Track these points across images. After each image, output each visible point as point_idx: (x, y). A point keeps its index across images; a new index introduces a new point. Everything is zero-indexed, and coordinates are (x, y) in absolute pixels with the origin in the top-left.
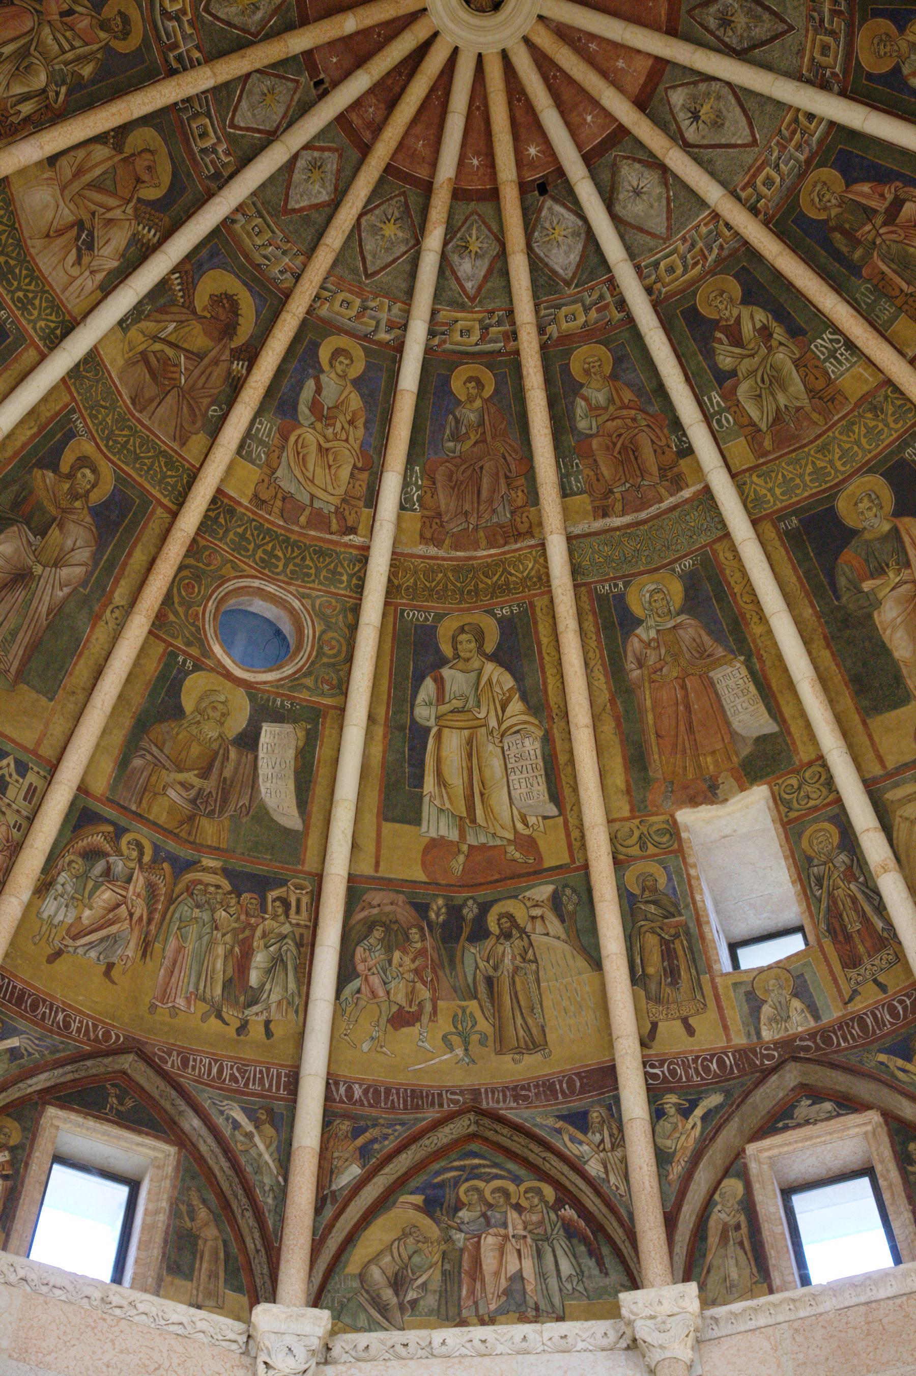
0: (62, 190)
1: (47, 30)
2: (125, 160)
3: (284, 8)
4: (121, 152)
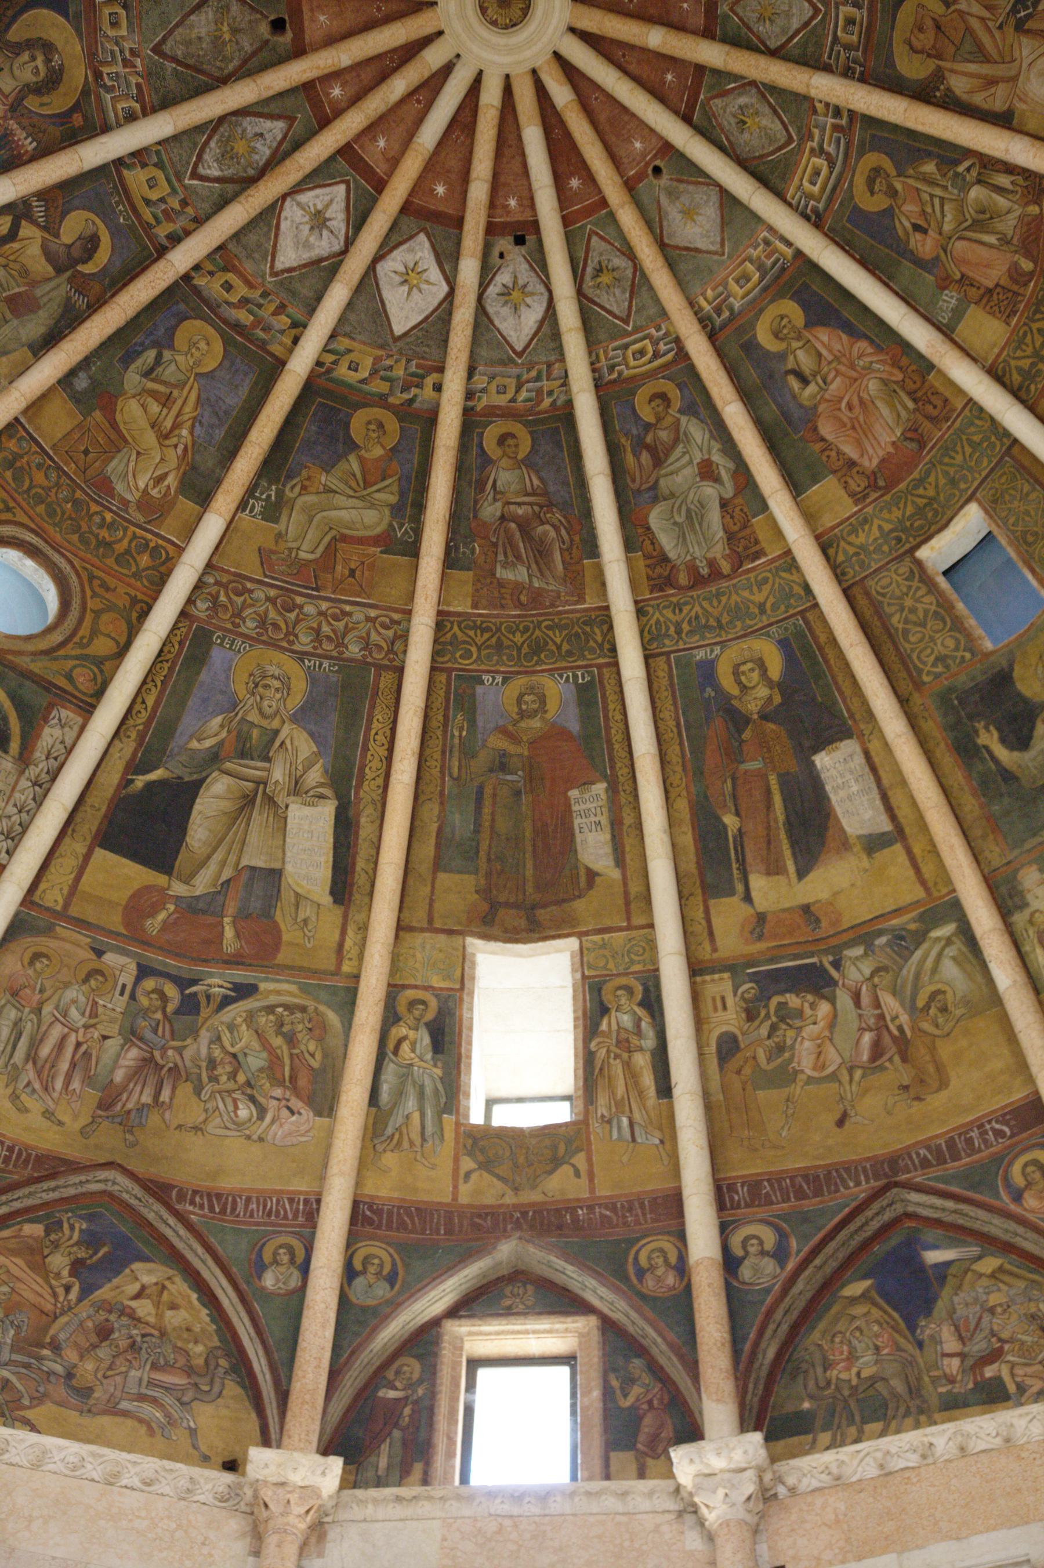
0: (1014, 79)
1: (947, 227)
2: (939, 57)
3: (715, 92)
4: (939, 69)
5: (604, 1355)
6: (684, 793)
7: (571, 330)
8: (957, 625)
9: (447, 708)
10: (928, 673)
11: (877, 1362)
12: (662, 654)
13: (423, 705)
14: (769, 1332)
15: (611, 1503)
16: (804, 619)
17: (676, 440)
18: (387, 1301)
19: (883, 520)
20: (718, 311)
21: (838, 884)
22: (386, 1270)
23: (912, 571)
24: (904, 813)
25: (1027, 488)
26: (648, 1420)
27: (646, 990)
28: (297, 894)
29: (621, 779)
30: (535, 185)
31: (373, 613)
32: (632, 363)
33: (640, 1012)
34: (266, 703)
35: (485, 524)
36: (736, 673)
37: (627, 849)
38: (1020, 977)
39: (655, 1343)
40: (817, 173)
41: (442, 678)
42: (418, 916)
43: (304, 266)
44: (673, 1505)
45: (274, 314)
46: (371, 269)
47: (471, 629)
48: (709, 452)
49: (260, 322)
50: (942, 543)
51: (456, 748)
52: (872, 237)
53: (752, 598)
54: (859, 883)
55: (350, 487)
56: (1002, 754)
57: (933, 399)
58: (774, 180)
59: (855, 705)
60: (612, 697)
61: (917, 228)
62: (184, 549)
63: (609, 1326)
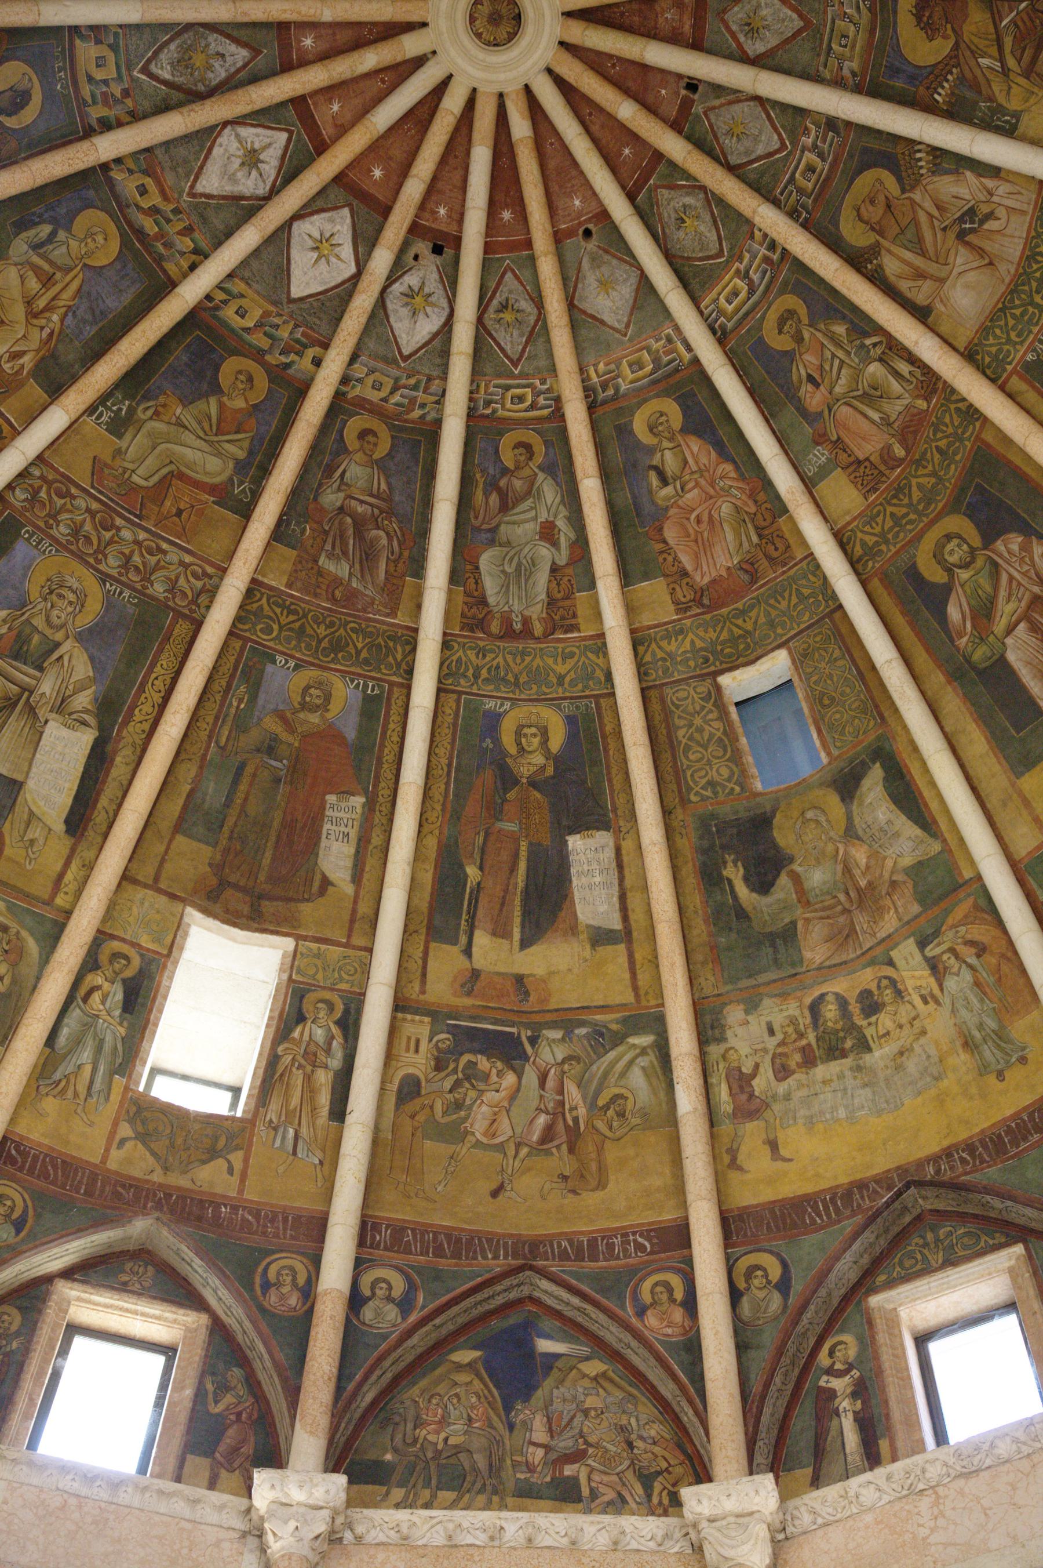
0: (942, 281)
1: (838, 390)
2: (881, 233)
5: (206, 1356)
6: (437, 832)
7: (462, 353)
8: (736, 757)
9: (232, 676)
10: (697, 794)
11: (466, 1433)
12: (453, 692)
13: (211, 666)
14: (374, 1377)
15: (179, 1507)
16: (597, 704)
17: (528, 493)
18: (9, 1246)
19: (697, 637)
20: (604, 386)
21: (557, 965)
22: (15, 1216)
23: (710, 692)
24: (637, 916)
25: (837, 653)
26: (231, 1432)
27: (347, 1011)
28: (31, 813)
29: (381, 799)
30: (469, 203)
31: (188, 559)
32: (509, 405)
33: (335, 1030)
34: (55, 612)
35: (322, 510)
36: (519, 733)
37: (367, 869)
38: (702, 1108)
39: (261, 1358)
40: (736, 294)
41: (238, 644)
42: (145, 873)
43: (224, 197)
44: (240, 1524)
45: (180, 233)
46: (287, 226)
47: (279, 606)
48: (555, 516)
49: (162, 236)
50: (745, 676)
51: (231, 718)
52: (768, 373)
53: (554, 667)
54: (576, 971)
55: (203, 429)
56: (742, 891)
57: (777, 541)
58: (694, 284)
59: (621, 800)
60: (394, 718)
61: (810, 379)
62: (19, 433)
63: (218, 1329)
